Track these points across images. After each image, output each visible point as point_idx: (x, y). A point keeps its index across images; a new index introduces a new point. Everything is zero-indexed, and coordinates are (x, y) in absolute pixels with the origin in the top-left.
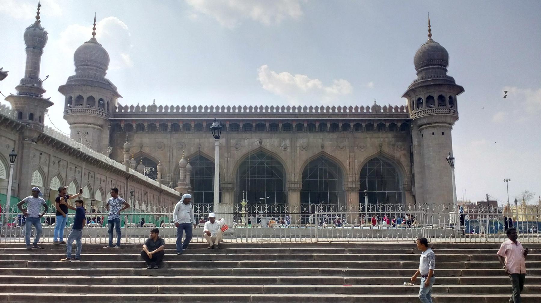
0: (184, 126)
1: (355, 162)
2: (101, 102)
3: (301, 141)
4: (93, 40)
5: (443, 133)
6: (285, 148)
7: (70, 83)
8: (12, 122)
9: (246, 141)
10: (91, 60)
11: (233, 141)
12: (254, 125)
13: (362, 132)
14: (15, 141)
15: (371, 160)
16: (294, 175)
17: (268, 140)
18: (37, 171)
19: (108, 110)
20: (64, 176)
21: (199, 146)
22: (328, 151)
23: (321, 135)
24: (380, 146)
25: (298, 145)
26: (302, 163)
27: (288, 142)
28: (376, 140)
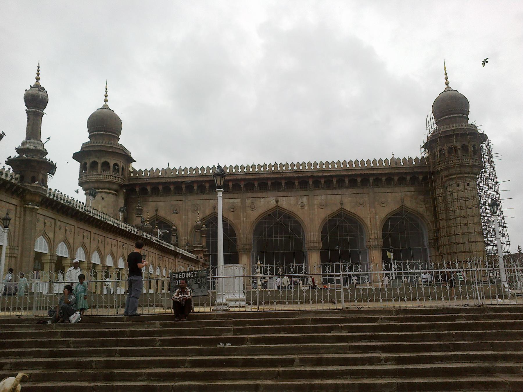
0: (198, 187)
1: (376, 218)
2: (117, 167)
3: (319, 198)
4: (106, 107)
6: (303, 206)
7: (84, 150)
8: (13, 185)
9: (261, 200)
10: (104, 126)
11: (248, 201)
12: (269, 183)
13: (383, 187)
14: (16, 205)
15: (393, 215)
16: (313, 234)
17: (284, 199)
18: (41, 236)
19: (122, 174)
20: (71, 241)
22: (348, 207)
23: (340, 191)
24: (402, 200)
25: (316, 203)
28: (397, 194)
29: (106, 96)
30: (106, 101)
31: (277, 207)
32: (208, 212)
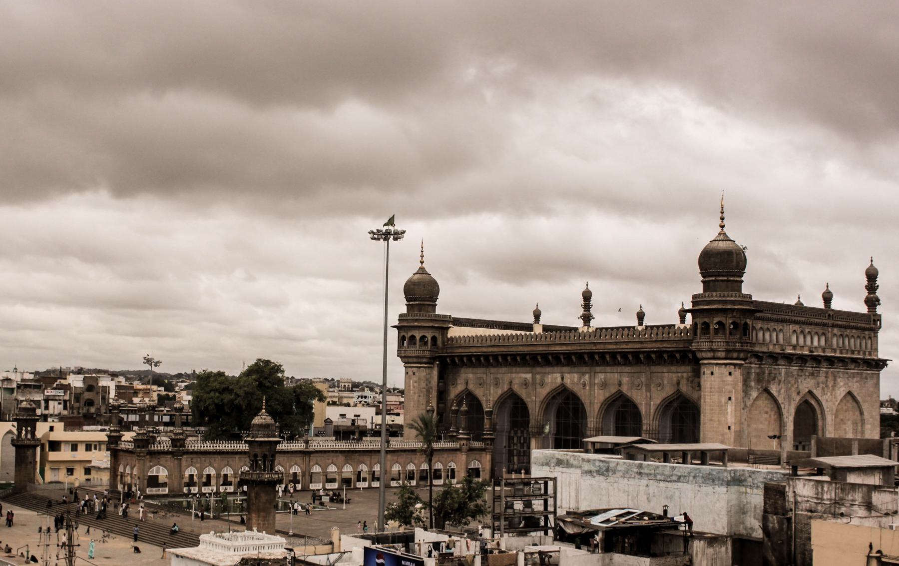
6: (584, 385)
21: (511, 383)
22: (625, 389)
24: (678, 383)
26: (599, 405)
27: (587, 376)
28: (674, 375)
29: (422, 257)
30: (422, 263)
31: (563, 385)
32: (506, 388)
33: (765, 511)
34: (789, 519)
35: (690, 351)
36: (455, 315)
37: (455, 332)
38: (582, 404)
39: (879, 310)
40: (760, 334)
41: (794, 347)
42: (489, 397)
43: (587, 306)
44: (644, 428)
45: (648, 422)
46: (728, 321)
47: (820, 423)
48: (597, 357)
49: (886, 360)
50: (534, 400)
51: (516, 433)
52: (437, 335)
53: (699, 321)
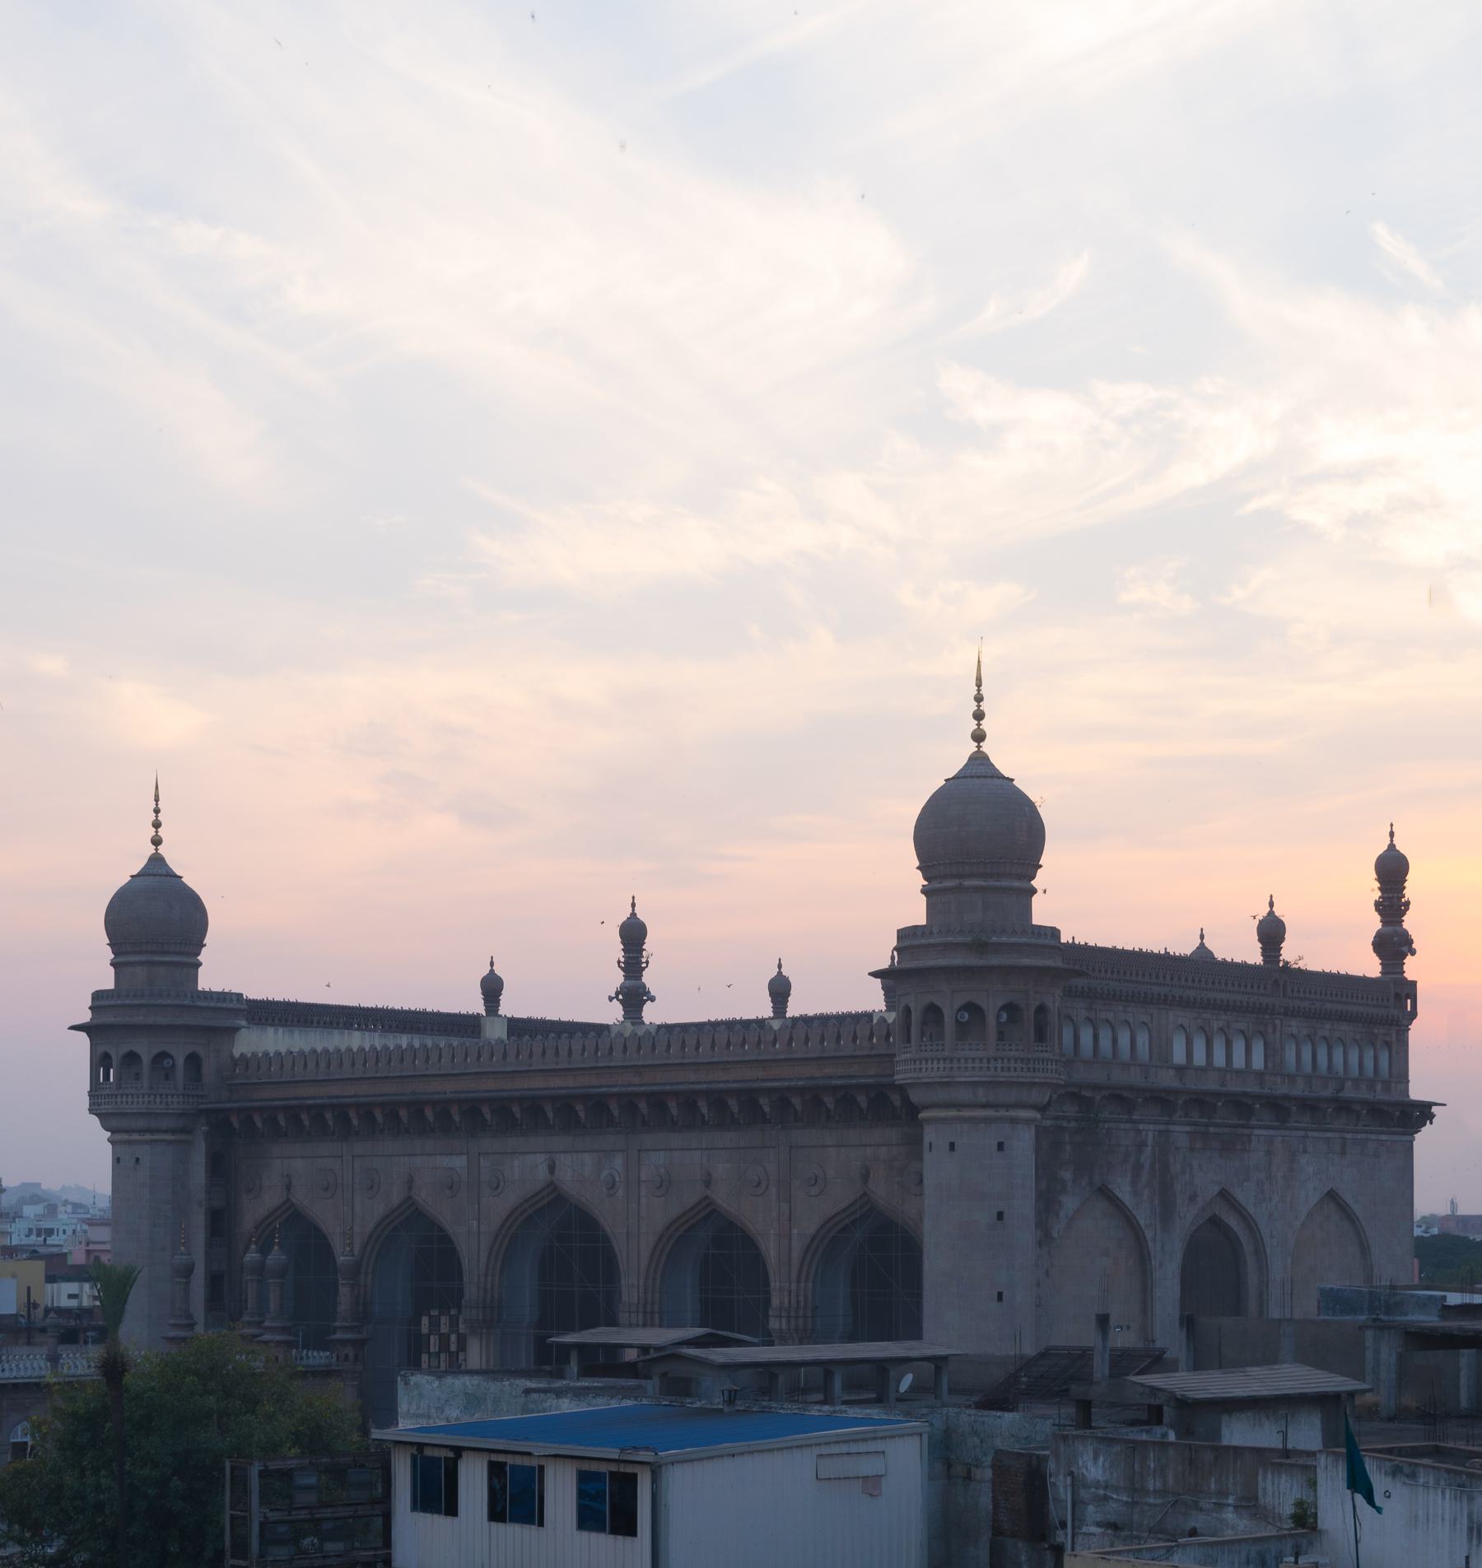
2: (167, 1063)
5: (952, 1146)
9: (516, 1163)
22: (722, 1197)
25: (643, 1176)
27: (618, 1162)
31: (552, 1186)
33: (997, 1531)
34: (1058, 1550)
35: (893, 1087)
36: (255, 991)
37: (252, 1042)
38: (606, 1239)
39: (1412, 968)
40: (1086, 1037)
41: (1180, 1070)
42: (349, 1221)
43: (633, 963)
44: (775, 1302)
45: (784, 1289)
46: (991, 1006)
47: (1252, 1279)
48: (643, 1106)
49: (1430, 1105)
50: (474, 1234)
51: (435, 1324)
52: (201, 1051)
53: (917, 1005)
